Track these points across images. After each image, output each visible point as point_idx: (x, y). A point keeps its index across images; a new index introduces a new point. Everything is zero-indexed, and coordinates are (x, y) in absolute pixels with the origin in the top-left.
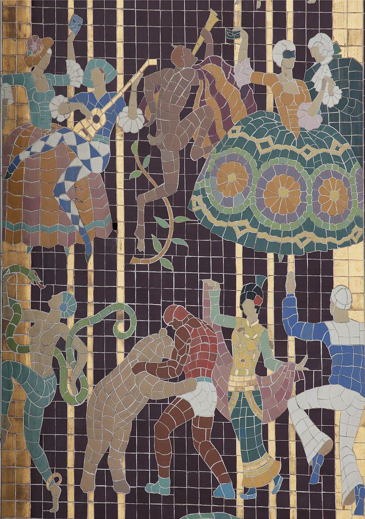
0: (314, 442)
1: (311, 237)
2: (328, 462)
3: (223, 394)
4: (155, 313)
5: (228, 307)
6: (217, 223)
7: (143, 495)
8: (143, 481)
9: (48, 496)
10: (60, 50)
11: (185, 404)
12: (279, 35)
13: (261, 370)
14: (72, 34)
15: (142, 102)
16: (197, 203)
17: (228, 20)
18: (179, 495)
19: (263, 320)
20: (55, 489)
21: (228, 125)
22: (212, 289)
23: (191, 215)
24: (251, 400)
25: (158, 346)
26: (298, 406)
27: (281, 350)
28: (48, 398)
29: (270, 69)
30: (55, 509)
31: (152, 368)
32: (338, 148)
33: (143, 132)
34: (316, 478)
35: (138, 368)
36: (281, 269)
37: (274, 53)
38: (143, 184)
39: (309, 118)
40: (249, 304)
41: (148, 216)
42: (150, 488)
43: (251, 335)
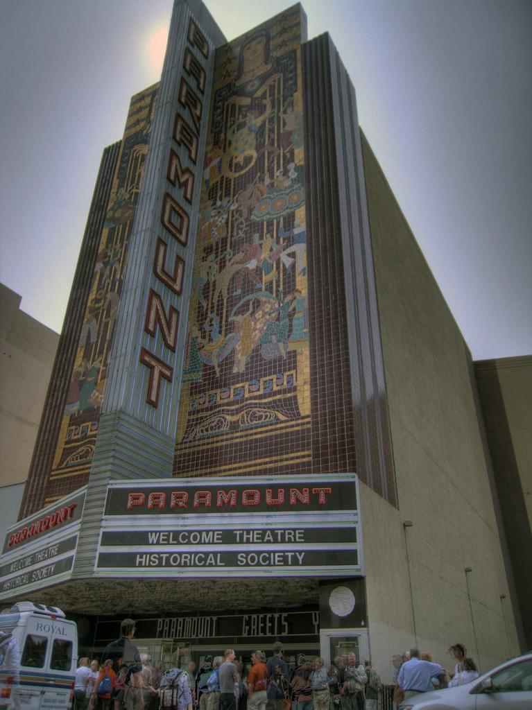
0: (287, 261)
1: (289, 210)
2: (293, 266)
3: (259, 261)
4: (239, 249)
5: (261, 238)
6: (258, 219)
7: (232, 296)
8: (232, 292)
9: (203, 307)
10: (216, 200)
11: (247, 268)
12: (278, 168)
13: (271, 250)
14: (219, 195)
15: (237, 201)
16: (253, 217)
17: (263, 173)
18: (244, 292)
19: (272, 237)
20: (205, 304)
21: (262, 195)
22: (256, 236)
23: (250, 221)
24: (268, 259)
25: (240, 256)
28: (205, 282)
29: (275, 177)
30: (205, 309)
31: (237, 263)
32: (296, 186)
33: (237, 208)
34: (289, 271)
35: (233, 264)
36: (278, 223)
37: (277, 173)
38: (236, 220)
39: (287, 183)
40: (268, 235)
41: (238, 226)
42: (234, 294)
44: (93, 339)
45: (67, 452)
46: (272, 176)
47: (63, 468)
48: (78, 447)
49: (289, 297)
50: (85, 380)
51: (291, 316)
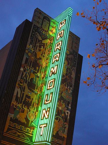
0: (67, 114)
2: (67, 116)
5: (63, 102)
26: (66, 111)
27: (66, 107)
37: (69, 87)
43: (64, 106)
44: (19, 96)
45: (9, 129)
46: (67, 87)
47: (8, 134)
48: (13, 130)
49: (65, 123)
50: (16, 109)
51: (65, 128)
